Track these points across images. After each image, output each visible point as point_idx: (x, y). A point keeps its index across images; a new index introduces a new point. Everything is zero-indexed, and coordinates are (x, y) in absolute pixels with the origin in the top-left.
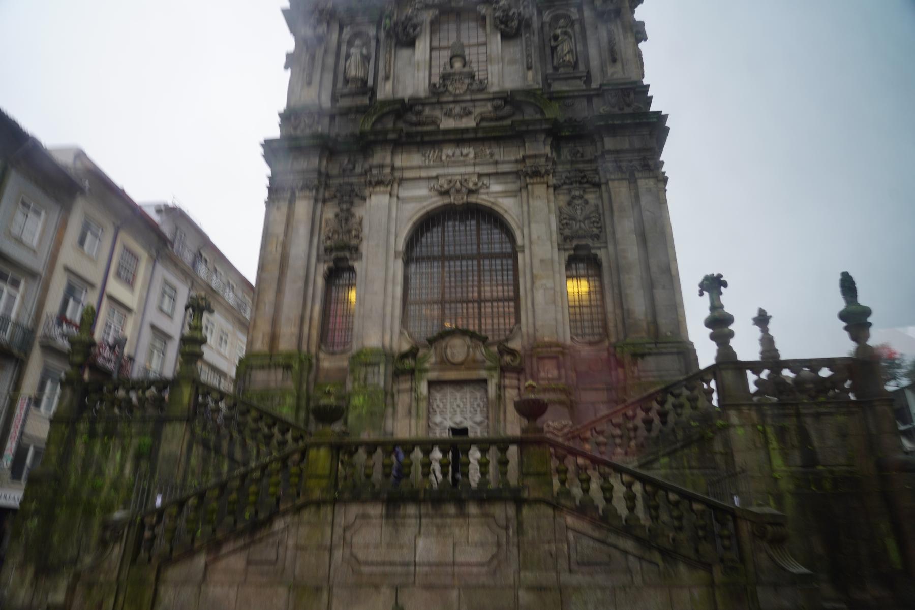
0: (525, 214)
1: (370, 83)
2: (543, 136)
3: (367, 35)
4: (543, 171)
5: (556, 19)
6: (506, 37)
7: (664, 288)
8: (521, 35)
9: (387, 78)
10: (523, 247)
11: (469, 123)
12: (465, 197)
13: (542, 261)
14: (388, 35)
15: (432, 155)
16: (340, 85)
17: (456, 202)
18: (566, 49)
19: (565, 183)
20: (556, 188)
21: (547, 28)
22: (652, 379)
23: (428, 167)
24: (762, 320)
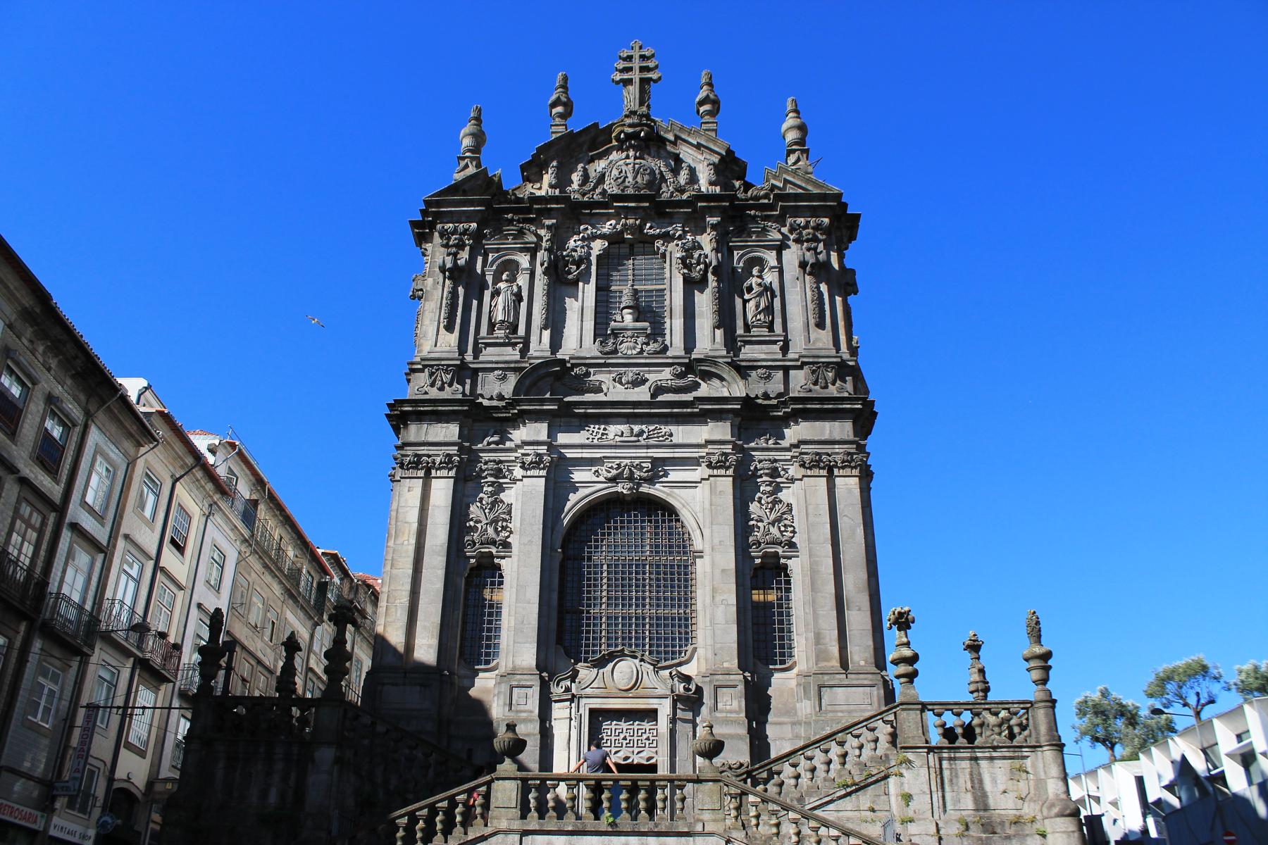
1: (521, 331)
7: (859, 610)
11: (642, 394)
13: (723, 571)
17: (625, 492)
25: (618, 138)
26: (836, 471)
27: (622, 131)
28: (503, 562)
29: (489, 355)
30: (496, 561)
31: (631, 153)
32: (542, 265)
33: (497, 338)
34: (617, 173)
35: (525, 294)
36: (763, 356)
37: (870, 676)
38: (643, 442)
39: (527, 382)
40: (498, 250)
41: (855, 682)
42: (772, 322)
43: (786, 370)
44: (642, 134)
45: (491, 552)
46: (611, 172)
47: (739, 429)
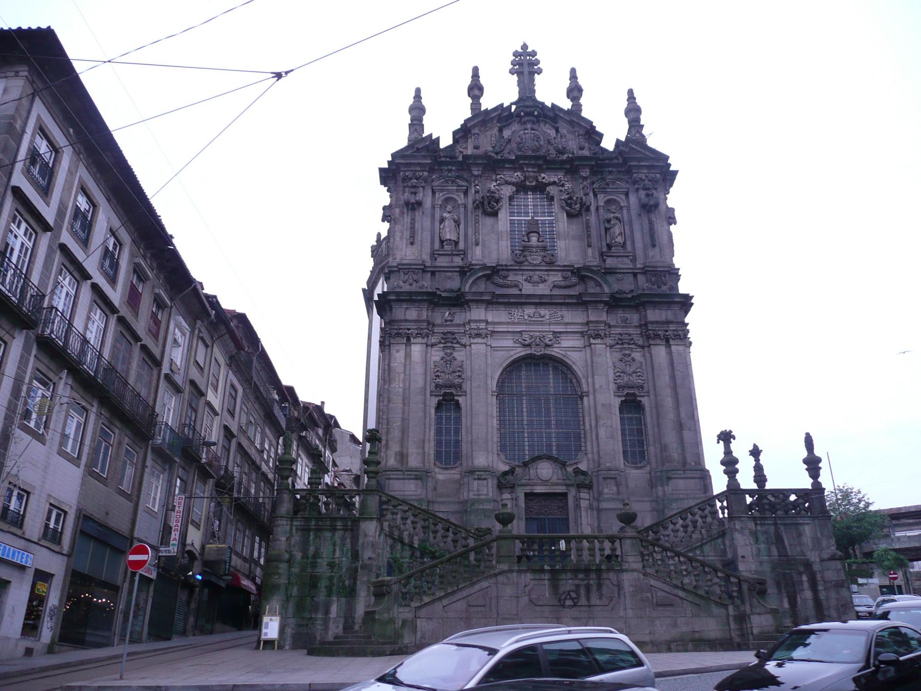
0: (589, 367)
1: (461, 245)
2: (603, 305)
3: (456, 200)
4: (602, 335)
5: (609, 202)
6: (570, 215)
7: (690, 429)
8: (582, 215)
9: (477, 244)
10: (588, 392)
12: (543, 349)
13: (603, 405)
14: (476, 208)
15: (517, 313)
16: (437, 245)
18: (617, 232)
19: (618, 343)
20: (611, 347)
21: (601, 211)
22: (681, 496)
23: (513, 323)
24: (755, 452)
25: (518, 116)
26: (672, 342)
27: (522, 111)
28: (461, 399)
29: (442, 262)
30: (456, 398)
31: (529, 126)
32: (474, 202)
33: (445, 251)
35: (462, 221)
36: (621, 266)
37: (699, 472)
38: (548, 321)
39: (471, 281)
40: (442, 191)
41: (690, 476)
42: (624, 243)
43: (635, 275)
44: (536, 113)
45: (452, 393)
47: (607, 313)
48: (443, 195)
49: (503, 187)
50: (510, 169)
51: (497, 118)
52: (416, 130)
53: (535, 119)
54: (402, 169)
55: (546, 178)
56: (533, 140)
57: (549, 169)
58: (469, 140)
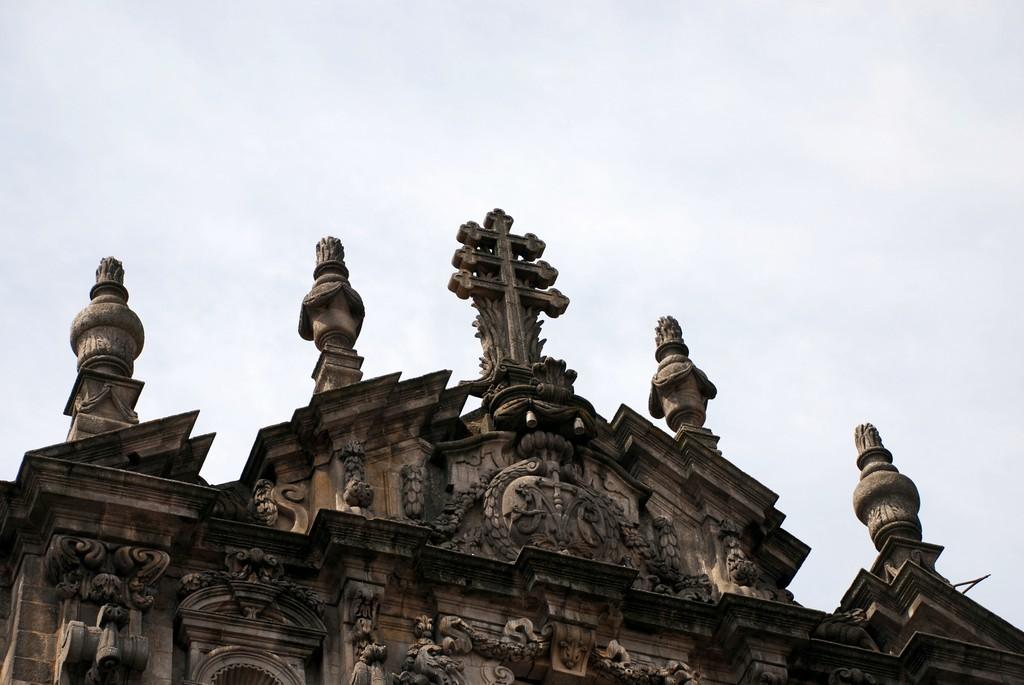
34: (520, 504)
40: (217, 637)
44: (578, 423)
46: (499, 498)
48: (225, 657)
49: (465, 662)
50: (490, 598)
51: (421, 418)
52: (109, 398)
53: (568, 444)
54: (61, 523)
55: (627, 657)
56: (574, 514)
57: (637, 628)
58: (320, 476)
